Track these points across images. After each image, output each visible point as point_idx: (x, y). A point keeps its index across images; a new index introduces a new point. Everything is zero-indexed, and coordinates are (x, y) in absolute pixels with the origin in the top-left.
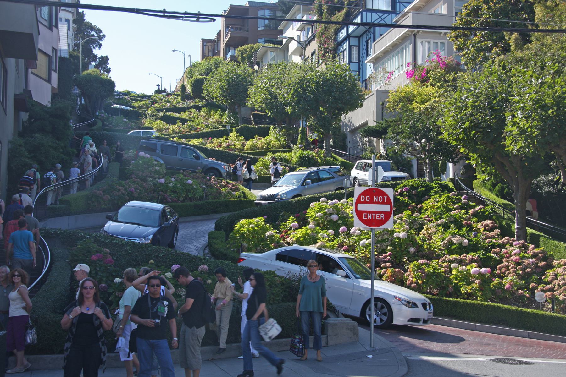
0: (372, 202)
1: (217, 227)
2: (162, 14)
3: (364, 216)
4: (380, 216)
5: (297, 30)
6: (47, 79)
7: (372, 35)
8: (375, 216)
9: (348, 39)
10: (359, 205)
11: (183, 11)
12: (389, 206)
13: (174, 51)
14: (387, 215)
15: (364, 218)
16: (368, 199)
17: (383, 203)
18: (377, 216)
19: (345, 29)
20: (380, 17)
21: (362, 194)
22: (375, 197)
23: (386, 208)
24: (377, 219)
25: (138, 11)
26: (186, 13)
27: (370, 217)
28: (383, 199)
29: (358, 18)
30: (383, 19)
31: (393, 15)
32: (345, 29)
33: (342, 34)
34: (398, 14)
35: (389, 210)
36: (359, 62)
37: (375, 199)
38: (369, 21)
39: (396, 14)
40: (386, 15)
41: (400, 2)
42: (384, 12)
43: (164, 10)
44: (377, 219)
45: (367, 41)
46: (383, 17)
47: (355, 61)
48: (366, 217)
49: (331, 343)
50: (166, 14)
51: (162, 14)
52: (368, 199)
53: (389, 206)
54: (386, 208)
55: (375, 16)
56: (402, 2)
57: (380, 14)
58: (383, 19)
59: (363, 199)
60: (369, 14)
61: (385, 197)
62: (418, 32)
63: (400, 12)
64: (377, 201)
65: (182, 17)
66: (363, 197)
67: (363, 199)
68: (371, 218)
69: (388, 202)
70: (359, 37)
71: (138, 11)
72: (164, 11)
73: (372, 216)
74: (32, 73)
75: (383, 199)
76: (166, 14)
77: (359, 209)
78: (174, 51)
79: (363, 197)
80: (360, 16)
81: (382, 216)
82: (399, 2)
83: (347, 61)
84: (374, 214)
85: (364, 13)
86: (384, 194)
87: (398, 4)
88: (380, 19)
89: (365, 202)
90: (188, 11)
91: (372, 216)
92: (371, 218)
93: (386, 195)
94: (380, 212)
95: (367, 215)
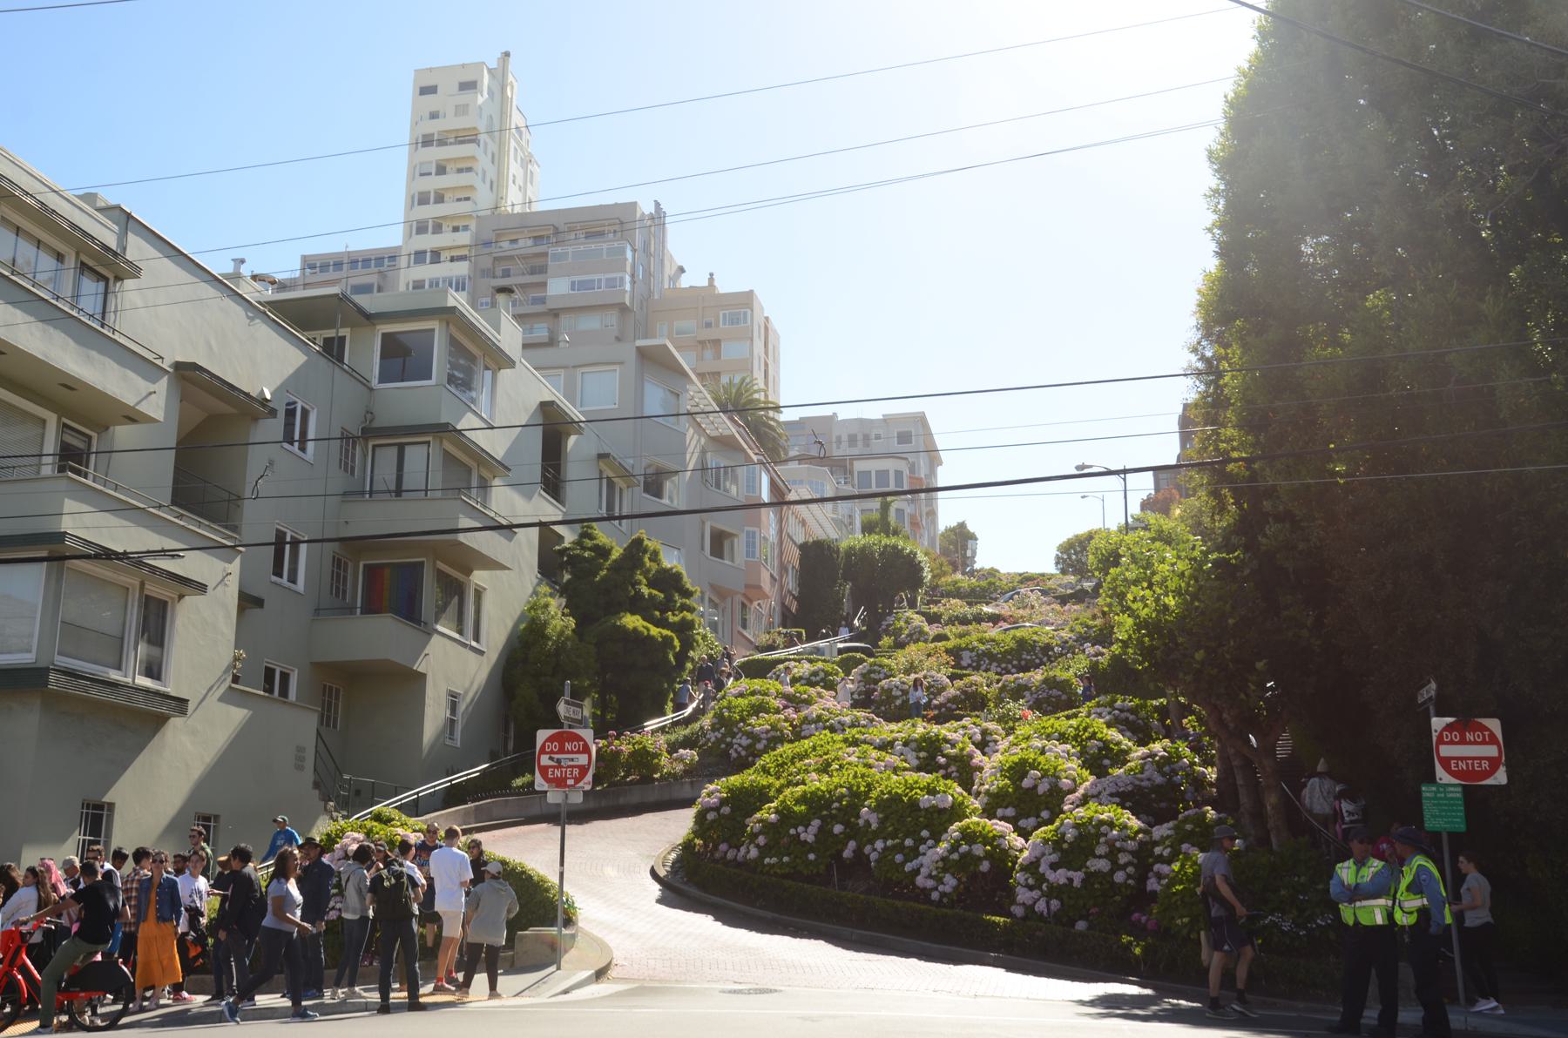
3: (550, 773)
12: (587, 755)
15: (550, 776)
16: (555, 747)
18: (568, 773)
21: (547, 741)
22: (567, 744)
28: (579, 745)
35: (586, 763)
37: (568, 746)
48: (553, 774)
52: (555, 747)
53: (587, 755)
61: (581, 743)
68: (559, 775)
73: (562, 772)
75: (579, 745)
86: (579, 738)
91: (562, 772)
92: (559, 775)
93: (583, 740)
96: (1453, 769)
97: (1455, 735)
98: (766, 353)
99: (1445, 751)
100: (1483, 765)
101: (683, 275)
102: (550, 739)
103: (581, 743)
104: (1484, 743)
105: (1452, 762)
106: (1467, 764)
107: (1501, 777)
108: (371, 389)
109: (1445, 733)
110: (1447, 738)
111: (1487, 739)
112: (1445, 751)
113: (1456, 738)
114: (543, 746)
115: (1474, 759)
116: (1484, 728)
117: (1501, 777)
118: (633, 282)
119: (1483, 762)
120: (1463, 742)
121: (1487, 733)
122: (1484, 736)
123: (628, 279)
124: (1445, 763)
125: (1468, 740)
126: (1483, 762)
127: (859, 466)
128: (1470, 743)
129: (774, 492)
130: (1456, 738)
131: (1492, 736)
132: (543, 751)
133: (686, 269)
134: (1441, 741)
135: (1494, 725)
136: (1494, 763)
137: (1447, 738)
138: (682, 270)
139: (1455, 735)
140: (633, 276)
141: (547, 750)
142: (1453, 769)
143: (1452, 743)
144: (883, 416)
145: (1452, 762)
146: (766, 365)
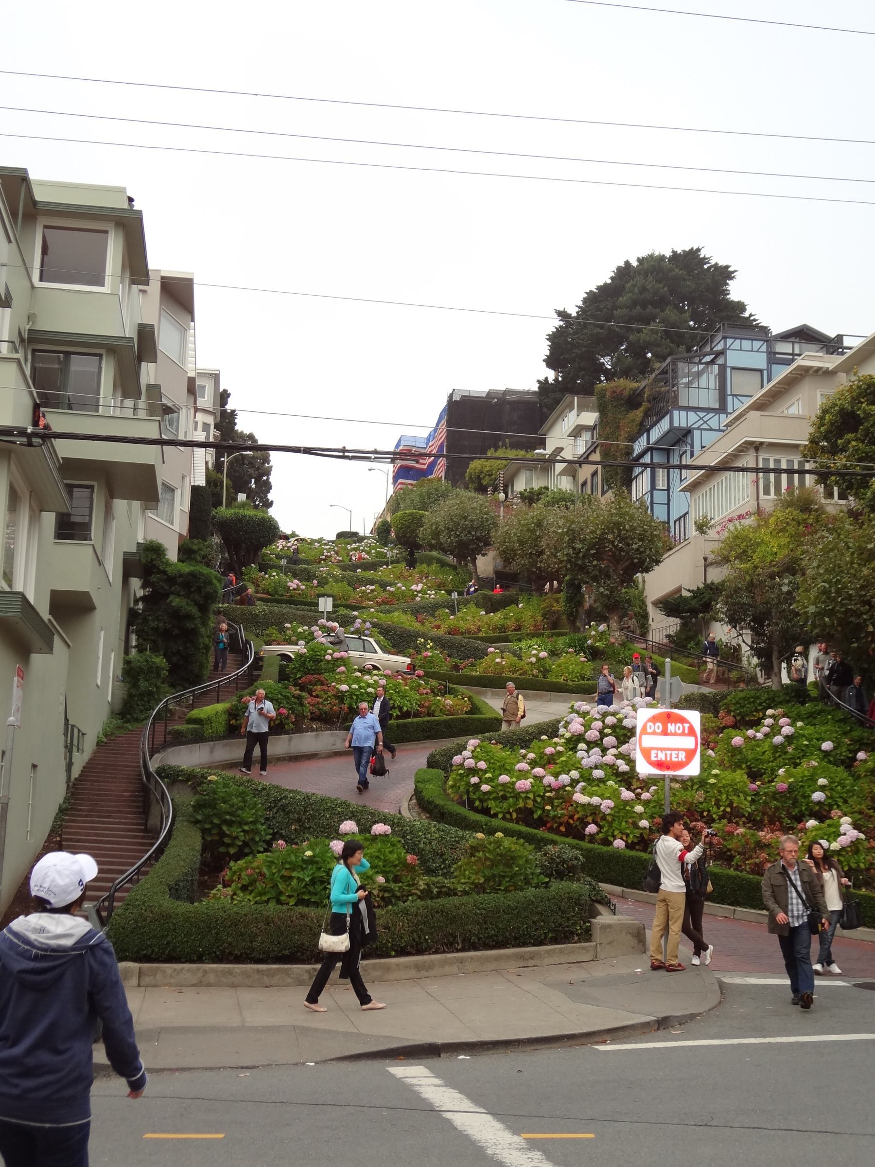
0: (665, 733)
1: (432, 763)
2: (341, 454)
4: (678, 755)
5: (569, 436)
7: (688, 446)
8: (671, 755)
9: (649, 454)
10: (644, 737)
11: (372, 449)
13: (370, 470)
14: (690, 754)
17: (683, 734)
18: (674, 756)
19: (645, 435)
20: (701, 418)
21: (649, 720)
22: (669, 724)
25: (307, 451)
26: (375, 452)
27: (662, 756)
29: (666, 418)
30: (705, 422)
31: (723, 416)
32: (645, 435)
33: (640, 445)
34: (730, 413)
36: (668, 490)
37: (671, 728)
38: (684, 425)
39: (728, 414)
40: (711, 415)
41: (733, 395)
42: (708, 410)
43: (344, 448)
45: (681, 456)
46: (705, 419)
47: (661, 487)
48: (657, 756)
49: (601, 955)
50: (346, 454)
51: (341, 454)
53: (692, 739)
55: (693, 417)
56: (736, 396)
57: (702, 414)
58: (705, 422)
59: (650, 728)
60: (683, 413)
61: (686, 725)
62: (762, 443)
63: (734, 411)
64: (673, 731)
65: (369, 458)
67: (650, 728)
69: (692, 732)
70: (668, 452)
71: (307, 451)
72: (344, 450)
73: (666, 755)
76: (346, 454)
78: (370, 470)
80: (668, 415)
81: (682, 756)
82: (733, 395)
83: (647, 487)
84: (669, 752)
85: (676, 413)
86: (683, 720)
87: (730, 399)
88: (701, 422)
89: (654, 733)
90: (379, 449)
93: (687, 722)
94: (678, 750)
103: (686, 725)
108: (33, 287)
111: (686, 731)
114: (644, 727)
125: (669, 731)
132: (644, 731)
141: (649, 730)
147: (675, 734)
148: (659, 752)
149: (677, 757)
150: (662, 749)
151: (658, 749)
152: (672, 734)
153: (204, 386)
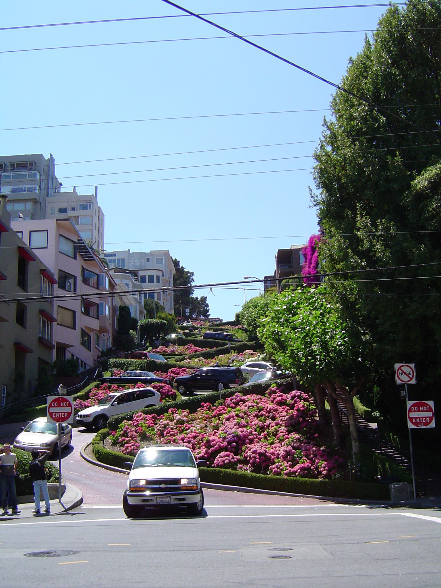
0: (59, 406)
3: (54, 415)
4: (64, 414)
6: (73, 327)
8: (61, 414)
18: (63, 415)
21: (52, 402)
22: (62, 403)
23: (68, 410)
24: (63, 416)
44: (63, 416)
53: (70, 408)
54: (68, 410)
61: (68, 403)
64: (63, 405)
66: (53, 404)
68: (58, 416)
73: (59, 415)
74: (58, 324)
77: (50, 411)
79: (53, 404)
81: (66, 415)
84: (60, 414)
89: (55, 407)
91: (59, 415)
93: (68, 401)
95: (55, 415)
96: (414, 422)
97: (416, 408)
98: (99, 223)
99: (412, 415)
100: (427, 420)
101: (61, 187)
102: (54, 401)
104: (427, 411)
105: (414, 419)
106: (420, 420)
107: (432, 425)
109: (412, 407)
110: (413, 409)
112: (412, 415)
113: (416, 409)
115: (423, 418)
116: (427, 405)
117: (432, 425)
118: (40, 189)
119: (427, 419)
120: (419, 411)
121: (428, 407)
122: (427, 408)
123: (38, 188)
124: (411, 419)
126: (427, 419)
127: (141, 274)
128: (421, 411)
129: (111, 286)
130: (416, 409)
131: (430, 408)
132: (50, 406)
133: (63, 184)
134: (410, 411)
135: (431, 403)
136: (431, 419)
137: (413, 409)
138: (61, 184)
139: (416, 408)
140: (40, 187)
142: (414, 422)
143: (415, 411)
144: (150, 251)
145: (414, 419)
146: (99, 227)
147: (64, 406)
148: (57, 414)
149: (64, 415)
150: (58, 413)
151: (56, 413)
152: (62, 407)
153: (162, 258)
